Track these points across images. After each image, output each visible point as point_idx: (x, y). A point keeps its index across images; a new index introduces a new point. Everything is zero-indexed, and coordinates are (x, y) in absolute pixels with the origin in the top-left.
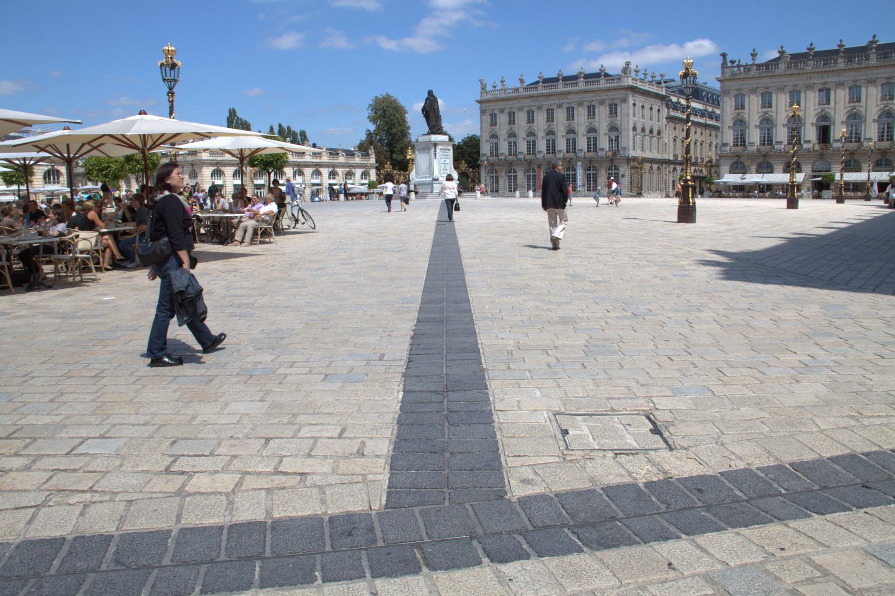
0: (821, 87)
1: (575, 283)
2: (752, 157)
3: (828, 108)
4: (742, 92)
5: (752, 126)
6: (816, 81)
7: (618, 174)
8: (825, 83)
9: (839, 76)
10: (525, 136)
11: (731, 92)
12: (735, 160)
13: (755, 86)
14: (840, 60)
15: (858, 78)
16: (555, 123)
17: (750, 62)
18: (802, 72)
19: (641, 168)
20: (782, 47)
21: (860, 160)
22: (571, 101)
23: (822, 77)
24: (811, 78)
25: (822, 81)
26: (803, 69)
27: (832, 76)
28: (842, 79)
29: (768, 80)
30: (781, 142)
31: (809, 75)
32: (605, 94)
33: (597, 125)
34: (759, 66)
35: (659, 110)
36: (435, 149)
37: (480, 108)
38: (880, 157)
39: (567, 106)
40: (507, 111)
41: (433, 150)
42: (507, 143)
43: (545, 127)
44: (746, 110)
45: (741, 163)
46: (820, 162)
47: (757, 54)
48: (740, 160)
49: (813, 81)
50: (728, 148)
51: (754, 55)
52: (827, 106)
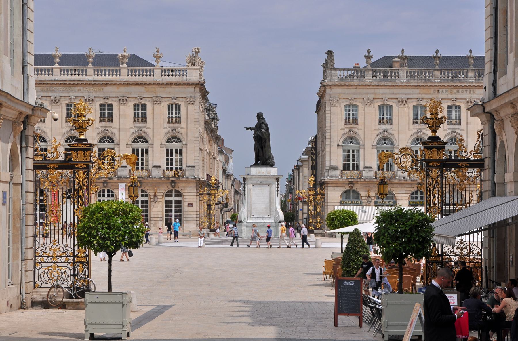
2: (368, 184)
3: (458, 129)
5: (368, 145)
6: (444, 96)
7: (180, 202)
9: (470, 93)
12: (347, 188)
13: (372, 96)
14: (471, 74)
18: (429, 84)
20: (368, 52)
24: (438, 92)
25: (450, 96)
27: (463, 92)
29: (386, 91)
30: (336, 167)
31: (437, 89)
32: (162, 89)
43: (64, 130)
44: (361, 125)
45: (354, 192)
48: (354, 188)
50: (337, 173)
51: (368, 57)
52: (457, 127)
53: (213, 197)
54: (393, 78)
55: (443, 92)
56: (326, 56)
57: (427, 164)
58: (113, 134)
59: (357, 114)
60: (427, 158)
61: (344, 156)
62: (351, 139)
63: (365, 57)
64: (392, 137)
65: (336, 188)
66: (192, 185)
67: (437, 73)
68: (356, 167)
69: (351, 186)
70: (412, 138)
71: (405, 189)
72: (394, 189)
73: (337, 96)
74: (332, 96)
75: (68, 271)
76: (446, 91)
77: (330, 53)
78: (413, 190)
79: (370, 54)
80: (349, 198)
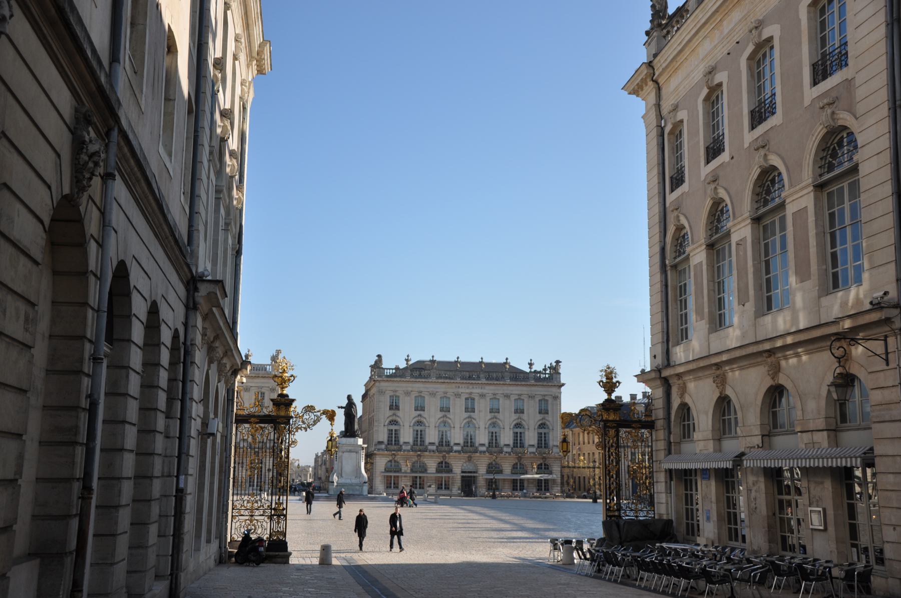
4: (397, 394)
5: (407, 425)
8: (471, 393)
9: (482, 388)
11: (387, 392)
12: (391, 458)
13: (410, 389)
15: (496, 392)
21: (502, 463)
23: (468, 388)
24: (459, 387)
25: (468, 391)
27: (476, 388)
28: (485, 391)
31: (457, 385)
38: (517, 461)
46: (467, 463)
48: (396, 459)
49: (461, 390)
50: (383, 446)
51: (407, 360)
56: (377, 358)
57: (605, 424)
59: (399, 403)
60: (604, 418)
62: (394, 422)
69: (394, 456)
74: (381, 388)
75: (264, 524)
77: (379, 356)
78: (439, 461)
79: (409, 358)
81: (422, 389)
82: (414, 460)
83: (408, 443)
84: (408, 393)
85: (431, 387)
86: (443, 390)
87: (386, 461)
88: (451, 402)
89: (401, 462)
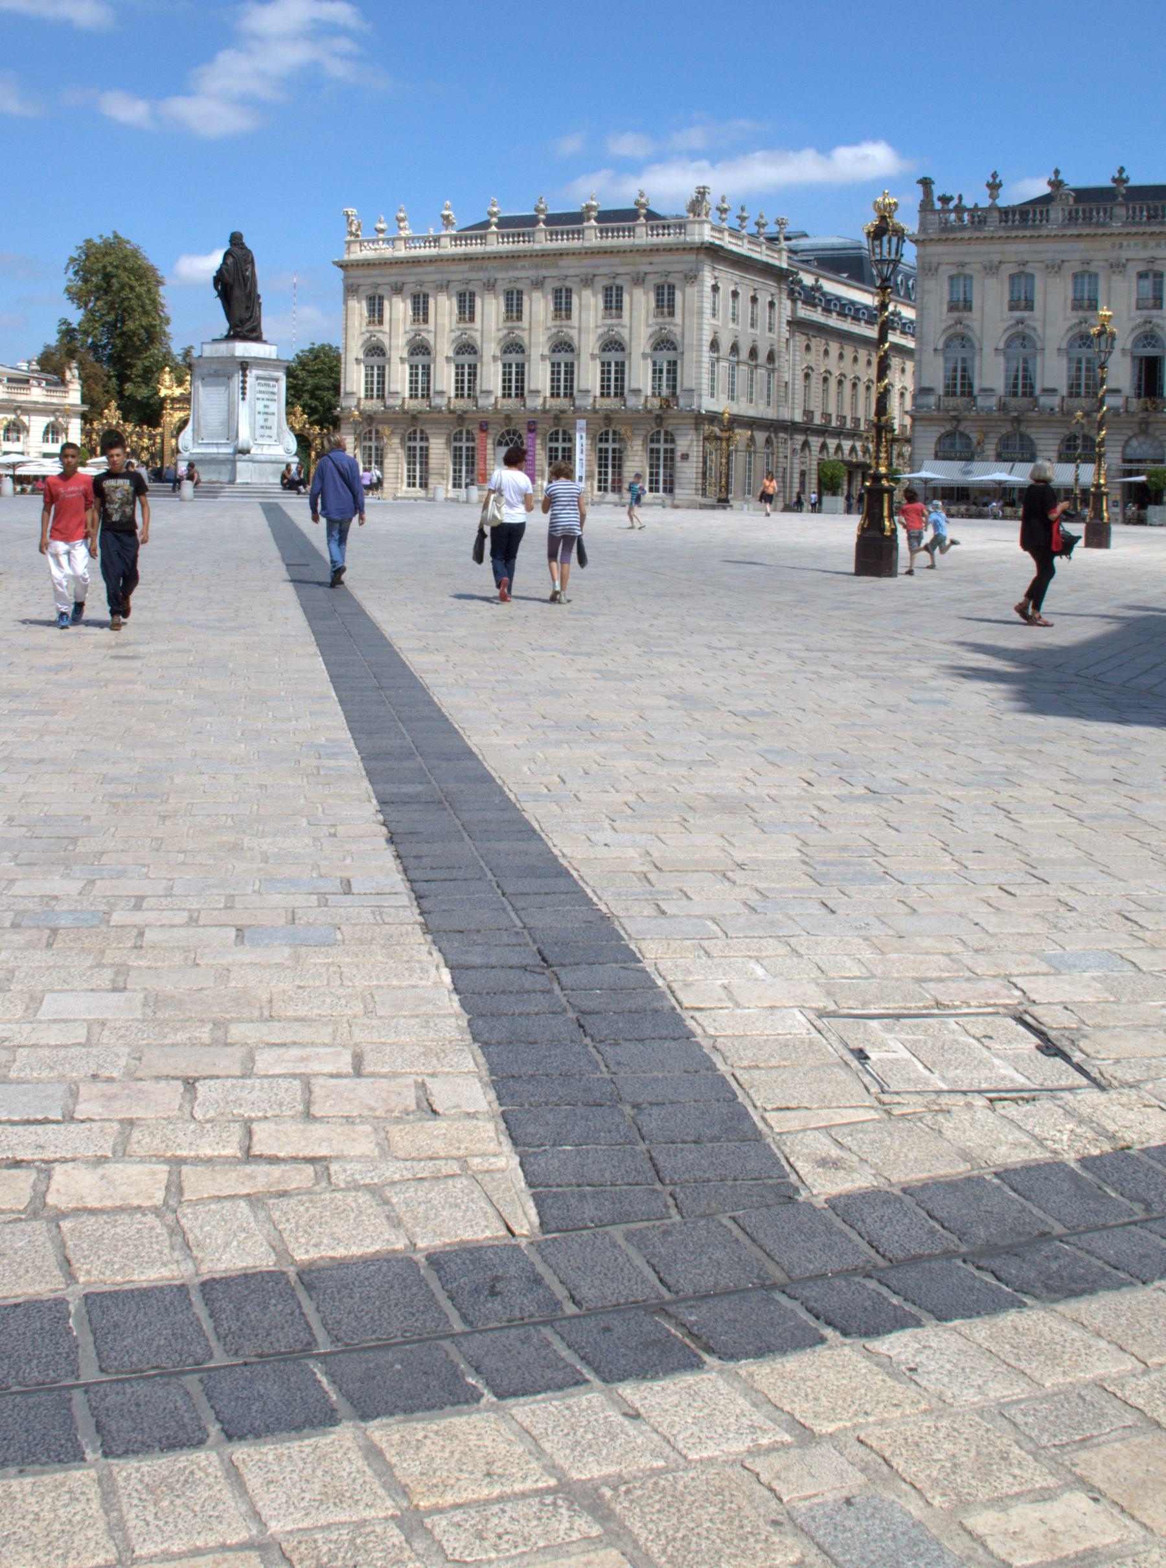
0: (1142, 267)
1: (697, 715)
3: (1158, 316)
4: (967, 271)
5: (988, 350)
6: (1130, 254)
7: (672, 451)
8: (1153, 260)
10: (451, 354)
11: (942, 268)
12: (948, 427)
13: (996, 258)
16: (525, 323)
17: (985, 203)
19: (728, 439)
20: (1057, 172)
22: (565, 272)
23: (1145, 246)
24: (1121, 246)
26: (1104, 225)
29: (1024, 247)
31: (1118, 240)
32: (646, 259)
33: (625, 333)
34: (1006, 213)
35: (772, 305)
36: (244, 375)
37: (346, 278)
39: (557, 284)
40: (409, 289)
41: (237, 378)
42: (407, 367)
44: (975, 314)
45: (962, 434)
46: (1141, 439)
47: (1000, 185)
48: (961, 429)
49: (1125, 254)
50: (931, 400)
51: (994, 187)
52: (1154, 312)
53: (724, 444)
54: (1037, 222)
55: (1128, 245)
58: (571, 338)
59: (971, 293)
61: (946, 370)
63: (989, 185)
64: (1032, 333)
65: (929, 428)
66: (688, 421)
67: (1120, 211)
68: (968, 390)
69: (955, 423)
70: (1070, 334)
71: (1054, 430)
72: (1033, 430)
73: (935, 260)
76: (1136, 245)
79: (997, 181)
80: (953, 445)
81: (1026, 257)
82: (1004, 431)
83: (992, 390)
84: (992, 269)
85: (1049, 250)
86: (1078, 256)
87: (938, 435)
88: (1102, 284)
89: (971, 435)
